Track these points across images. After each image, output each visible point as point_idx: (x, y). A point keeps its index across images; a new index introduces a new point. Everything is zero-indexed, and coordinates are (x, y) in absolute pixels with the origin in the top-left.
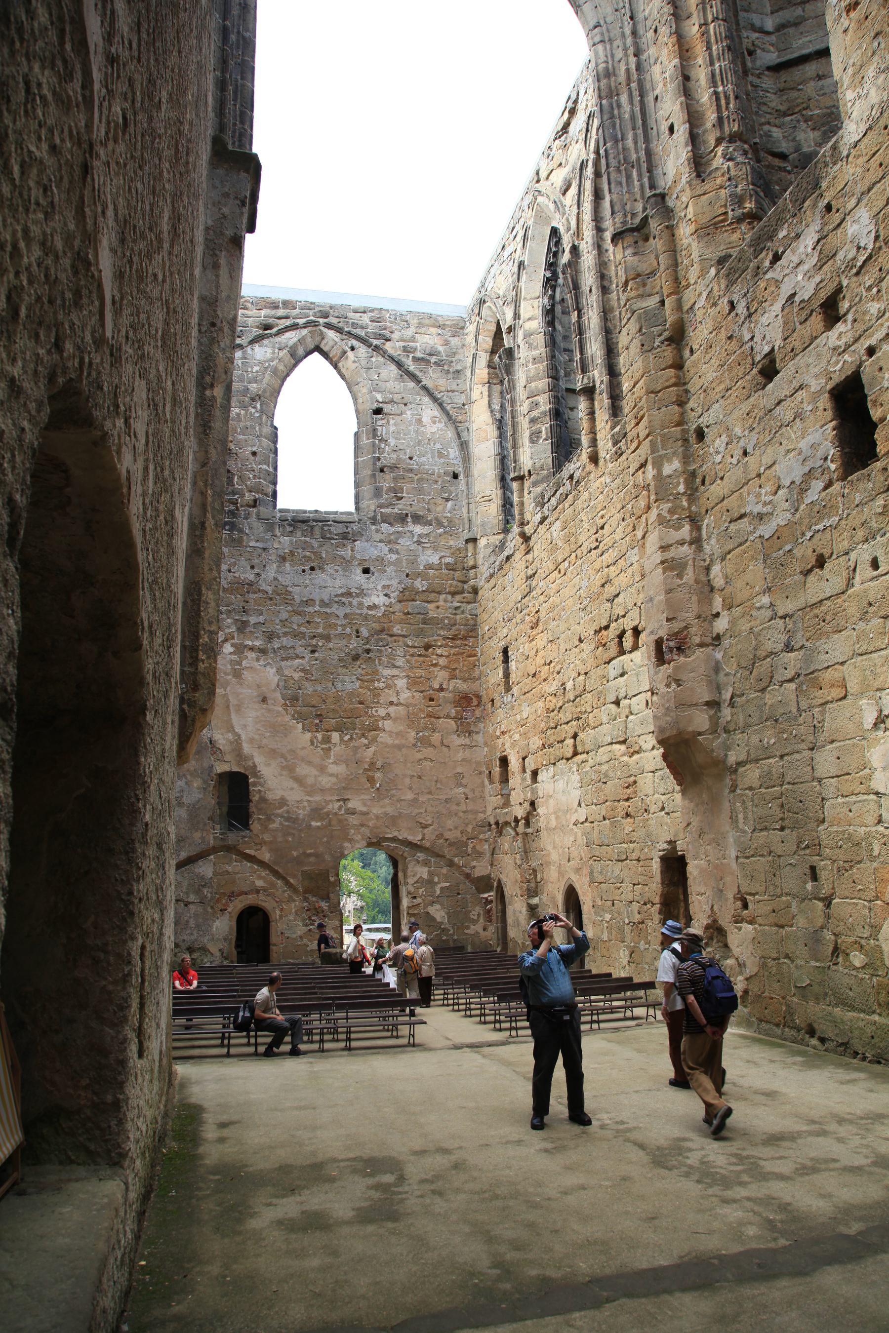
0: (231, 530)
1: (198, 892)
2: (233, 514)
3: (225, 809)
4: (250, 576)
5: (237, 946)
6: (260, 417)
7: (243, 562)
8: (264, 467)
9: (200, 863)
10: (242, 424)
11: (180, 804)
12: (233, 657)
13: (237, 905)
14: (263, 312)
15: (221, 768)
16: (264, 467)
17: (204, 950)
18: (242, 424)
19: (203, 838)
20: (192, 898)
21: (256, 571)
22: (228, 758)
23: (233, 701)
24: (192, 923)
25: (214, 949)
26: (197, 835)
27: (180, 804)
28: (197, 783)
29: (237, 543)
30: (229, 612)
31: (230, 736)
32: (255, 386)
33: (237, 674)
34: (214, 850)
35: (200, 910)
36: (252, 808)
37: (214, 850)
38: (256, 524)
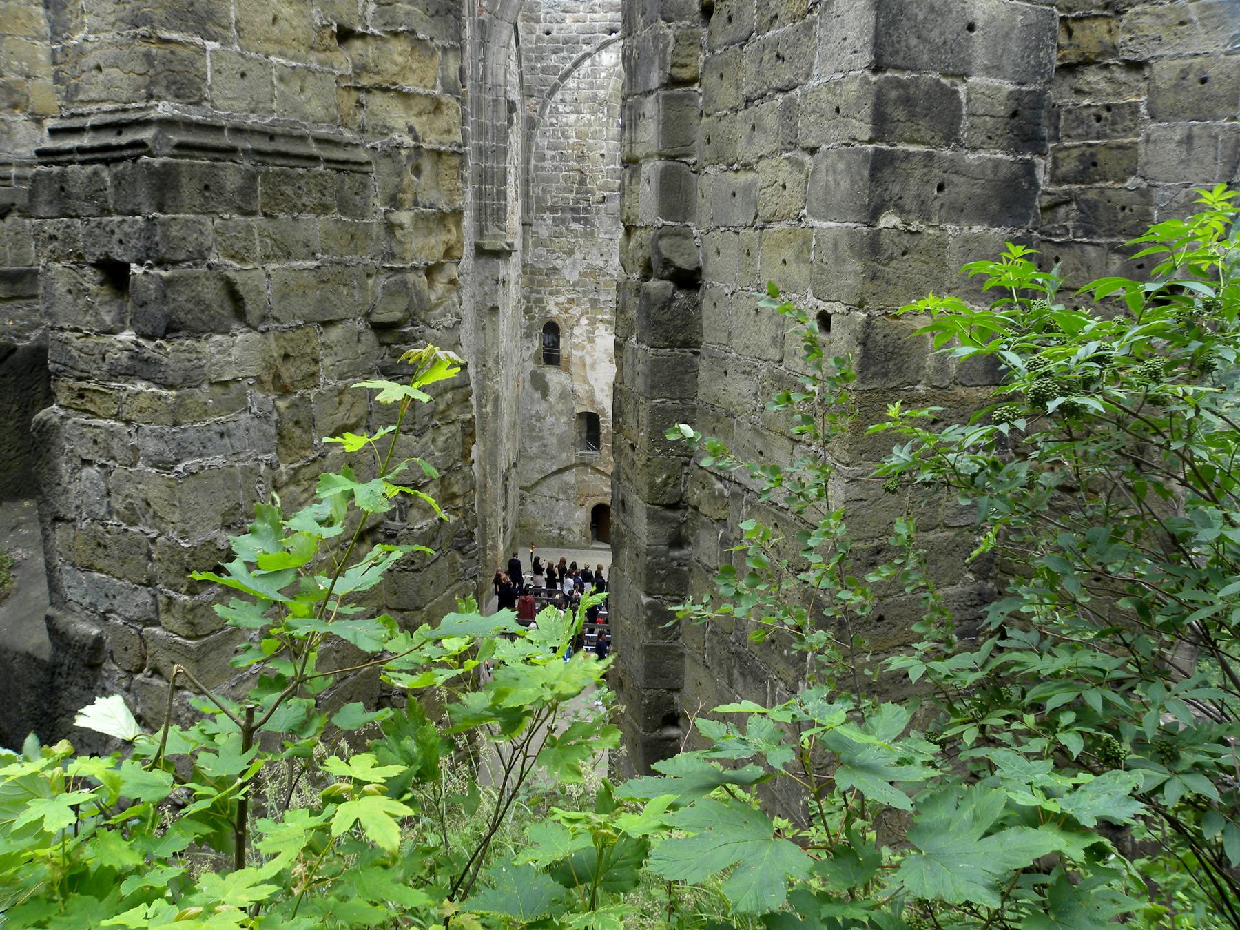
0: (585, 224)
1: (565, 492)
2: (585, 209)
3: (584, 435)
4: (601, 264)
5: (592, 527)
6: (607, 121)
7: (595, 251)
8: (612, 166)
9: (567, 473)
10: (592, 129)
11: (552, 434)
12: (589, 328)
13: (592, 502)
14: (609, 15)
15: (579, 409)
16: (612, 166)
17: (570, 530)
18: (592, 129)
19: (568, 458)
20: (561, 496)
21: (605, 258)
22: (585, 402)
23: (588, 361)
24: (561, 513)
25: (576, 529)
26: (564, 455)
27: (552, 434)
28: (564, 419)
29: (589, 235)
30: (584, 292)
31: (586, 387)
32: (602, 91)
33: (591, 341)
34: (576, 465)
35: (567, 504)
36: (602, 439)
37: (576, 465)
38: (605, 219)
